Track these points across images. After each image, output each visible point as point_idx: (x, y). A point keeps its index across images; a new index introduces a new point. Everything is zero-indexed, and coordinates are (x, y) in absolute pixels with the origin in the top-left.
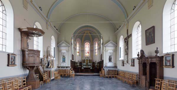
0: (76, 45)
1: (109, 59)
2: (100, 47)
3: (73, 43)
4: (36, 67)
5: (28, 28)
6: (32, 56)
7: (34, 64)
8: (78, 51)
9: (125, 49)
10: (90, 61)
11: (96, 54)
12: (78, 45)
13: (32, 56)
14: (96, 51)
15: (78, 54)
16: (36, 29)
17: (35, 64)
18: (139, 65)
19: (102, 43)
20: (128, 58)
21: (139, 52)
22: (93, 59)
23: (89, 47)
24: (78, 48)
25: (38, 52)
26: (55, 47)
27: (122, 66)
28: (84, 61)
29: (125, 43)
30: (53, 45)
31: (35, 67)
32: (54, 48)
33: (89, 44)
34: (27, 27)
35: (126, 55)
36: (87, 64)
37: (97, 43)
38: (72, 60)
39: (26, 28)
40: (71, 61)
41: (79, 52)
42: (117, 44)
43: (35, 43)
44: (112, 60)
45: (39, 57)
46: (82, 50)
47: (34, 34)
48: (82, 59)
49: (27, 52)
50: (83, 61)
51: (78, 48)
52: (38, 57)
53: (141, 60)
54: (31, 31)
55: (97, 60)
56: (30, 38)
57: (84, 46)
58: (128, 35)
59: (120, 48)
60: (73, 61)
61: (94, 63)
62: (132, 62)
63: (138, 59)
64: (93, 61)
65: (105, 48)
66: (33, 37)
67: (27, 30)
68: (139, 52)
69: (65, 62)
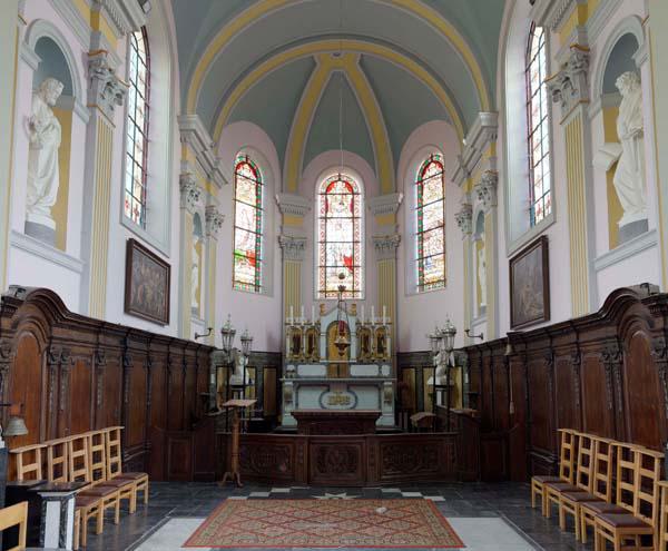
8: (244, 242)
10: (373, 342)
11: (434, 272)
15: (245, 273)
22: (395, 323)
24: (245, 215)
28: (304, 341)
36: (341, 369)
37: (433, 170)
41: (254, 260)
46: (292, 242)
50: (297, 340)
51: (245, 215)
57: (313, 200)
61: (406, 362)
64: (395, 343)
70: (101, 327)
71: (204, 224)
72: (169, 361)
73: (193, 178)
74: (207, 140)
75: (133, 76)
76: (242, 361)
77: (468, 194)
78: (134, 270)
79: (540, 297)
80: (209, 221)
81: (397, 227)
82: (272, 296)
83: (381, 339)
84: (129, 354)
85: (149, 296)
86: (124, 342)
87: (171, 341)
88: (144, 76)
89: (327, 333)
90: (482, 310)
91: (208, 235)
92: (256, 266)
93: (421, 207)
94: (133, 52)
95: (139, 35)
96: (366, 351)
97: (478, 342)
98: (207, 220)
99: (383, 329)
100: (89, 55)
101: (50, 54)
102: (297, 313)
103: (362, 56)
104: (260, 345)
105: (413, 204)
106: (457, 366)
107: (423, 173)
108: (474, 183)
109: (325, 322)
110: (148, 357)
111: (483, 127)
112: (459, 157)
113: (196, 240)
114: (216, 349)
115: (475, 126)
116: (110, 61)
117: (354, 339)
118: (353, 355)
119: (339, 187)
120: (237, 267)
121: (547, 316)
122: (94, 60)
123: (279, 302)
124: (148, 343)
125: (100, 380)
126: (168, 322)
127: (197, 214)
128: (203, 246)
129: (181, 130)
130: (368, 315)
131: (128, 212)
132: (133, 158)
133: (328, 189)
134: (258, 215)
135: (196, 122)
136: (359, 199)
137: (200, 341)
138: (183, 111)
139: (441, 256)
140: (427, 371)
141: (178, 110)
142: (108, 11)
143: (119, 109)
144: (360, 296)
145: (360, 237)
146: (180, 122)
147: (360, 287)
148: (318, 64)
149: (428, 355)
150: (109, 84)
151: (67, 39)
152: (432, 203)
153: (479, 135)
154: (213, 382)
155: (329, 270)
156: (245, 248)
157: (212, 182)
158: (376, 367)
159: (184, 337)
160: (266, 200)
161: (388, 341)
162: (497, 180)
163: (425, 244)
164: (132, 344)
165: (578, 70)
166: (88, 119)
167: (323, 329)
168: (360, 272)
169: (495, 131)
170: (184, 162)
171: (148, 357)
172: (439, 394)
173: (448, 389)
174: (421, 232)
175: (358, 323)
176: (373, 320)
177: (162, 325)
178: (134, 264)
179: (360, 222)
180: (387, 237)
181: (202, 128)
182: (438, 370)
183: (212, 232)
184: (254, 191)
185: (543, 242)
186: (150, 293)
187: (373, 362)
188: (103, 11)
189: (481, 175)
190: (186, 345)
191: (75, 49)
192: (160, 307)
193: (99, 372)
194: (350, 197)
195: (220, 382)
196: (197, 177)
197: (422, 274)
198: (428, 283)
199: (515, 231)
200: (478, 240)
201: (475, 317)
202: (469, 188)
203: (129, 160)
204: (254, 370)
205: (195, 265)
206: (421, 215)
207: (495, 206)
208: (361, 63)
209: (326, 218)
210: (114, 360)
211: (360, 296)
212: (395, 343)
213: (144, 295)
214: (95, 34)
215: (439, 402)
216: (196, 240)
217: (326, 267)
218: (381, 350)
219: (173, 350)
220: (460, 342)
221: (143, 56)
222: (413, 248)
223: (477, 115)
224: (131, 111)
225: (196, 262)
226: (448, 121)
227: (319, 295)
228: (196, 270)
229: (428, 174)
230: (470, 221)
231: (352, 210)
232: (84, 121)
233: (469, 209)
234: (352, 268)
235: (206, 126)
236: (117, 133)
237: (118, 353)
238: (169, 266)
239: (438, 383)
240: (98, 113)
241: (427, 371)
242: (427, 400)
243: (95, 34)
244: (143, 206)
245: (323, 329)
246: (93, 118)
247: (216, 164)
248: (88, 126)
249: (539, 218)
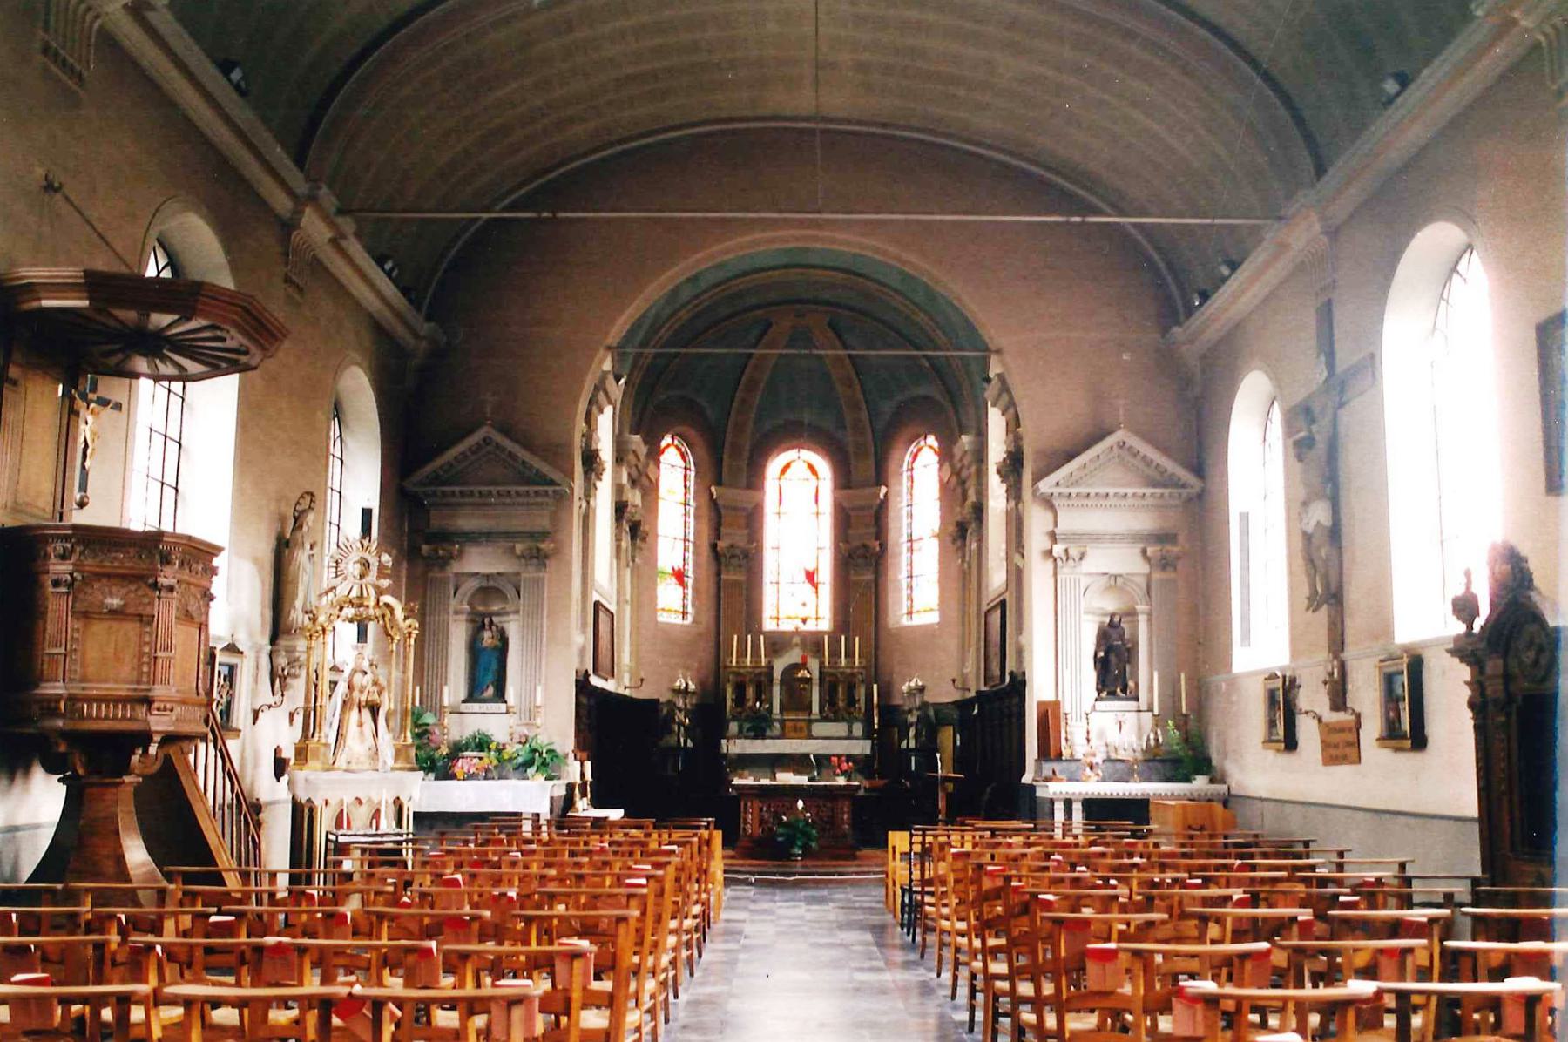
0: (646, 483)
1: (1102, 665)
2: (979, 510)
3: (606, 452)
4: (170, 739)
5: (95, 283)
6: (116, 614)
7: (141, 711)
9: (1307, 538)
13: (116, 614)
16: (182, 293)
17: (148, 702)
18: (1478, 729)
19: (997, 450)
20: (1337, 644)
21: (1468, 574)
25: (200, 555)
26: (375, 505)
27: (1269, 741)
29: (1298, 466)
30: (357, 479)
31: (145, 738)
32: (367, 513)
34: (88, 274)
35: (1314, 603)
38: (595, 681)
39: (69, 273)
40: (582, 685)
41: (680, 576)
42: (1199, 470)
43: (145, 456)
44: (1146, 675)
45: (203, 627)
47: (155, 345)
49: (64, 557)
52: (187, 617)
53: (1494, 665)
54: (129, 315)
55: (938, 678)
56: (111, 388)
58: (1331, 366)
59: (1244, 517)
60: (610, 686)
62: (1391, 699)
63: (1464, 650)
65: (1037, 522)
66: (137, 376)
67: (85, 303)
68: (1468, 574)
69: (500, 695)
83: (851, 688)
96: (833, 703)
102: (742, 654)
109: (779, 666)
118: (815, 708)
119: (799, 469)
130: (835, 653)
133: (784, 471)
167: (777, 674)
187: (843, 720)
218: (852, 701)
245: (777, 674)
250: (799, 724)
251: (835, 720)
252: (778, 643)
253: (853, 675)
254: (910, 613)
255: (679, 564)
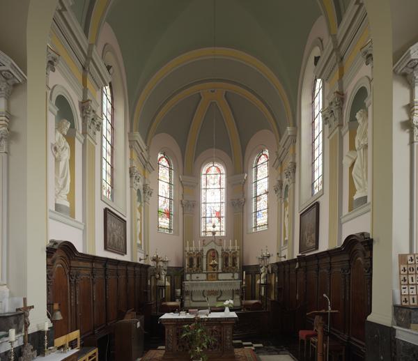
8: (164, 204)
10: (230, 260)
12: (164, 173)
14: (263, 204)
15: (164, 222)
22: (241, 250)
23: (223, 185)
24: (164, 189)
28: (194, 262)
33: (223, 171)
37: (263, 159)
41: (169, 214)
46: (188, 203)
48: (184, 251)
50: (191, 260)
51: (164, 189)
57: (199, 178)
61: (252, 271)
64: (242, 262)
70: (94, 259)
71: (142, 194)
72: (127, 274)
73: (136, 169)
74: (144, 147)
75: (105, 111)
76: (164, 273)
77: (281, 175)
78: (108, 225)
79: (314, 236)
80: (146, 193)
81: (244, 194)
82: (178, 235)
83: (234, 259)
84: (108, 272)
85: (116, 240)
86: (105, 266)
87: (127, 264)
88: (110, 110)
89: (207, 256)
90: (286, 242)
91: (145, 201)
92: (170, 218)
93: (256, 182)
94: (104, 96)
95: (108, 87)
96: (227, 265)
97: (283, 260)
98: (144, 193)
99: (235, 253)
100: (82, 103)
101: (62, 103)
102: (191, 245)
103: (226, 92)
104: (172, 264)
105: (252, 180)
106: (272, 273)
107: (258, 161)
108: (284, 169)
109: (206, 250)
110: (117, 273)
111: (289, 136)
112: (276, 152)
113: (139, 204)
114: (150, 266)
115: (284, 136)
116: (93, 105)
117: (220, 260)
118: (220, 268)
119: (213, 170)
120: (160, 219)
121: (317, 247)
122: (84, 105)
123: (182, 239)
124: (117, 265)
125: (94, 287)
126: (126, 253)
127: (138, 189)
128: (142, 209)
129: (130, 141)
130: (228, 244)
131: (104, 193)
132: (106, 160)
133: (207, 171)
134: (170, 188)
135: (138, 137)
136: (224, 177)
137: (142, 262)
138: (131, 131)
139: (266, 210)
140: (257, 276)
141: (128, 130)
142: (91, 75)
143: (98, 133)
144: (223, 234)
145: (224, 200)
146: (129, 136)
147: (223, 229)
148: (203, 98)
149: (258, 267)
150: (93, 119)
151: (72, 96)
152: (261, 177)
153: (286, 142)
154: (149, 284)
155: (208, 219)
156: (164, 207)
157: (147, 170)
158: (231, 274)
159: (134, 261)
160: (174, 179)
161: (238, 259)
162: (295, 167)
163: (258, 203)
164: (109, 267)
165: (337, 107)
166: (83, 141)
167: (205, 254)
168: (223, 220)
169: (295, 137)
170: (131, 159)
171: (117, 273)
172: (263, 288)
173: (267, 285)
174: (256, 197)
175: (222, 250)
176: (231, 248)
177: (123, 255)
178: (108, 222)
179: (224, 191)
180: (238, 200)
181: (141, 139)
182: (262, 275)
183: (147, 200)
184: (168, 174)
185: (317, 205)
186: (116, 237)
187: (231, 272)
188: (89, 75)
189: (288, 164)
190: (135, 265)
191: (75, 100)
192: (122, 247)
193: (94, 283)
194: (219, 175)
195: (153, 284)
196: (138, 168)
197: (256, 221)
198: (259, 226)
199: (302, 200)
200: (285, 201)
201: (282, 245)
202: (281, 171)
203: (104, 161)
204: (169, 277)
205: (138, 220)
206: (256, 186)
207: (294, 182)
208: (225, 96)
209: (206, 189)
210: (101, 276)
211: (223, 234)
212: (242, 262)
213: (114, 239)
214: (85, 91)
215: (263, 294)
216: (139, 204)
217: (206, 217)
218: (234, 264)
219: (129, 268)
220: (273, 260)
221: (110, 98)
222: (252, 205)
223: (286, 128)
224: (104, 133)
225: (139, 218)
226: (271, 130)
227: (203, 234)
228: (139, 222)
229: (260, 162)
230: (280, 189)
231: (220, 184)
232: (81, 142)
233: (281, 183)
234: (220, 218)
235: (143, 138)
236: (97, 148)
237: (103, 272)
238: (125, 221)
239: (262, 282)
240: (88, 137)
241: (257, 276)
242: (257, 291)
243: (85, 91)
244: (112, 188)
245: (205, 254)
246: (85, 140)
247: (149, 159)
248: (83, 145)
249: (316, 191)
250: (214, 274)
251: (228, 272)
252: (205, 241)
253: (235, 253)
254: (256, 227)
255: (218, 210)
